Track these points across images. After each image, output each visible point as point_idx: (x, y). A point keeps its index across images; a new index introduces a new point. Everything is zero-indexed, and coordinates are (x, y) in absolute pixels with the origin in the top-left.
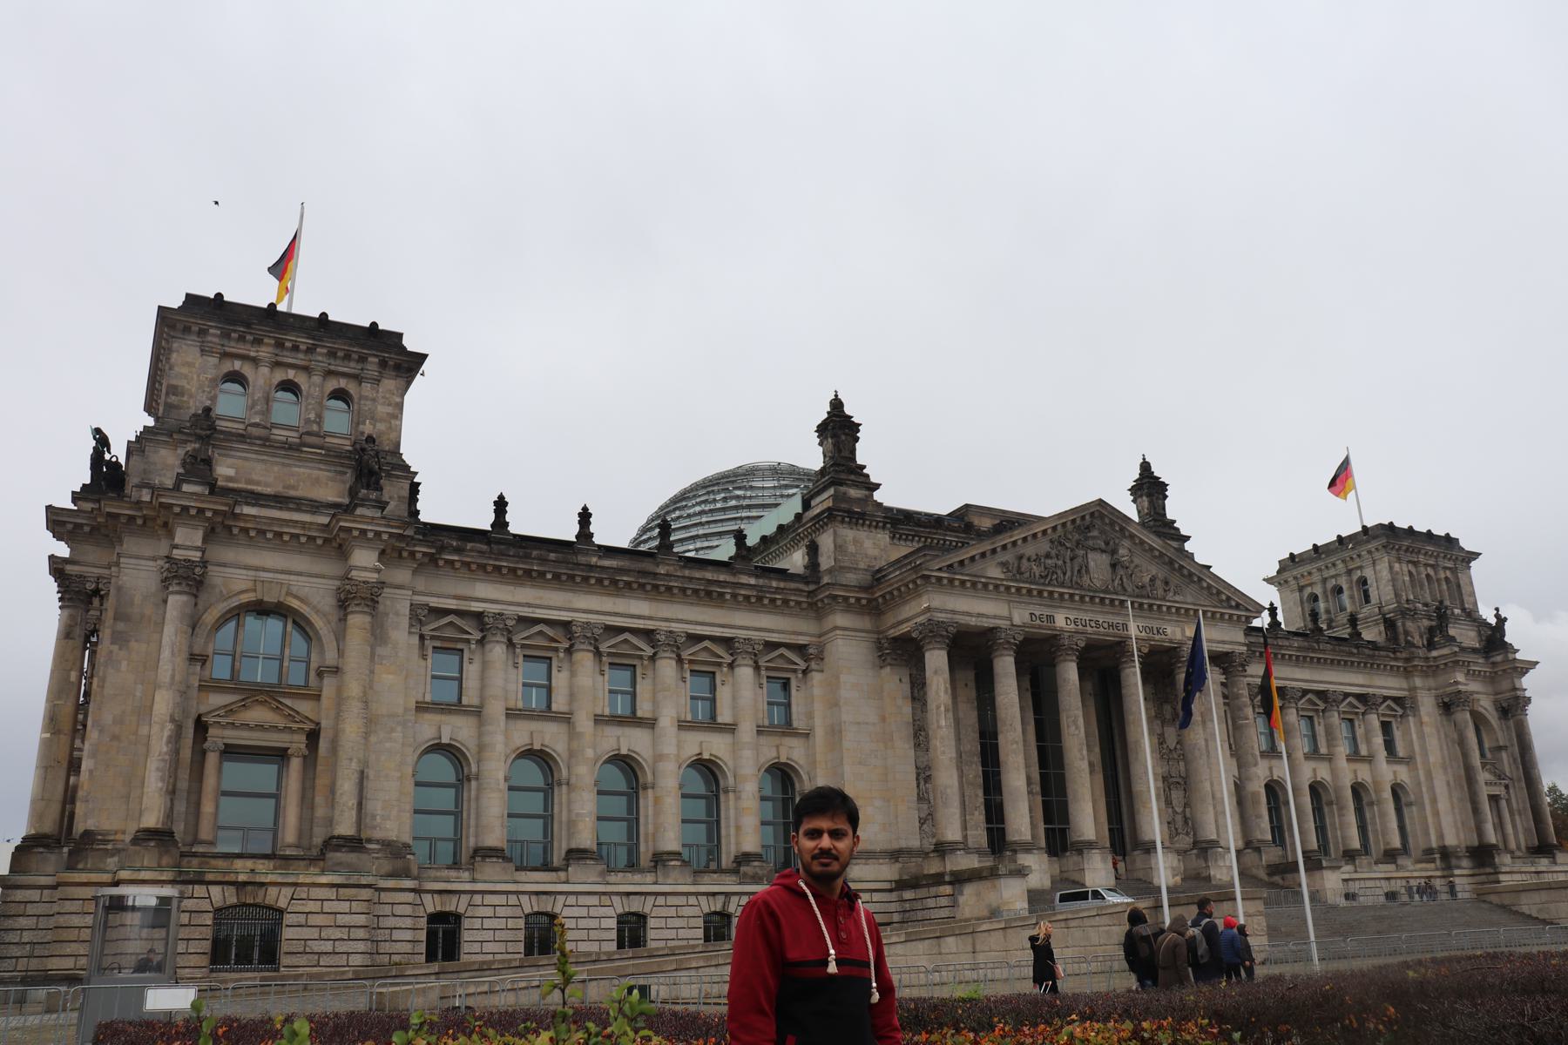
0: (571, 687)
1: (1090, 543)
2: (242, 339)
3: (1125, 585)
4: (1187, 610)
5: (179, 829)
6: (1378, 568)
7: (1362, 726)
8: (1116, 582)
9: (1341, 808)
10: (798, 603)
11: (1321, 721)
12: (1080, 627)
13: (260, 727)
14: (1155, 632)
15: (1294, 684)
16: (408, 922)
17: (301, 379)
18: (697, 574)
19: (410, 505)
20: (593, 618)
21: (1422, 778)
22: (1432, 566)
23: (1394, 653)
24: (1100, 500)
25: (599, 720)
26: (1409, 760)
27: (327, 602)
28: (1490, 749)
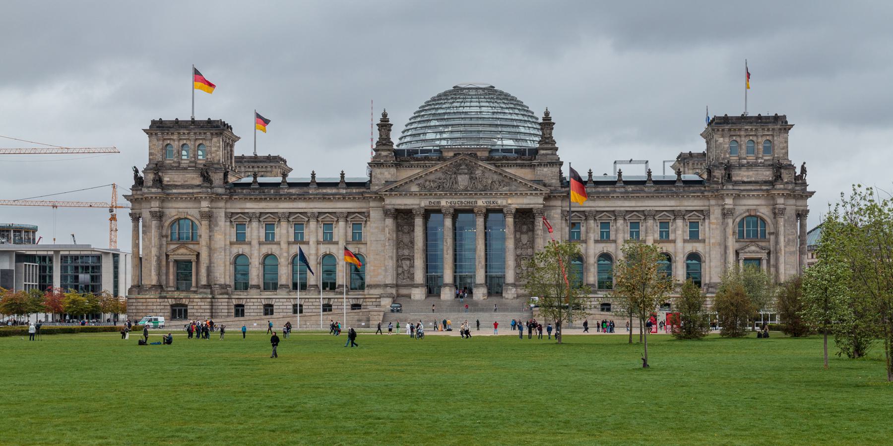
0: (280, 233)
2: (168, 134)
5: (164, 283)
7: (674, 225)
10: (359, 198)
13: (182, 254)
14: (492, 203)
15: (622, 209)
16: (226, 307)
17: (188, 142)
18: (324, 191)
19: (224, 179)
20: (285, 210)
21: (707, 250)
22: (755, 135)
23: (705, 187)
25: (289, 243)
26: (704, 241)
27: (198, 217)
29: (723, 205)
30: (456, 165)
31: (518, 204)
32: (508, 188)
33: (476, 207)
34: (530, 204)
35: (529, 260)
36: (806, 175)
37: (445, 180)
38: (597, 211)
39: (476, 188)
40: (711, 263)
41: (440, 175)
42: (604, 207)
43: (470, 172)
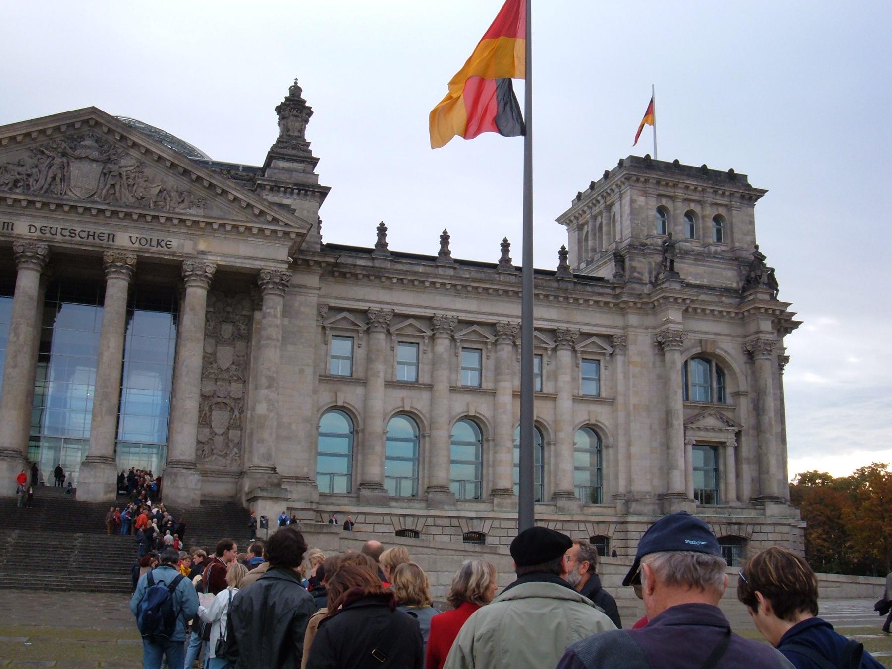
1: (77, 153)
3: (118, 194)
4: (196, 223)
6: (624, 201)
7: (554, 363)
8: (104, 191)
9: (495, 446)
11: (492, 355)
12: (48, 235)
14: (154, 243)
15: (450, 314)
21: (621, 419)
22: (698, 202)
23: (614, 289)
24: (93, 107)
26: (611, 402)
28: (731, 394)
29: (654, 328)
30: (71, 138)
31: (224, 255)
32: (201, 212)
33: (110, 248)
34: (256, 259)
35: (232, 410)
36: (777, 291)
37: (34, 170)
38: (397, 316)
39: (117, 199)
40: (634, 450)
41: (23, 155)
42: (412, 306)
43: (104, 157)
